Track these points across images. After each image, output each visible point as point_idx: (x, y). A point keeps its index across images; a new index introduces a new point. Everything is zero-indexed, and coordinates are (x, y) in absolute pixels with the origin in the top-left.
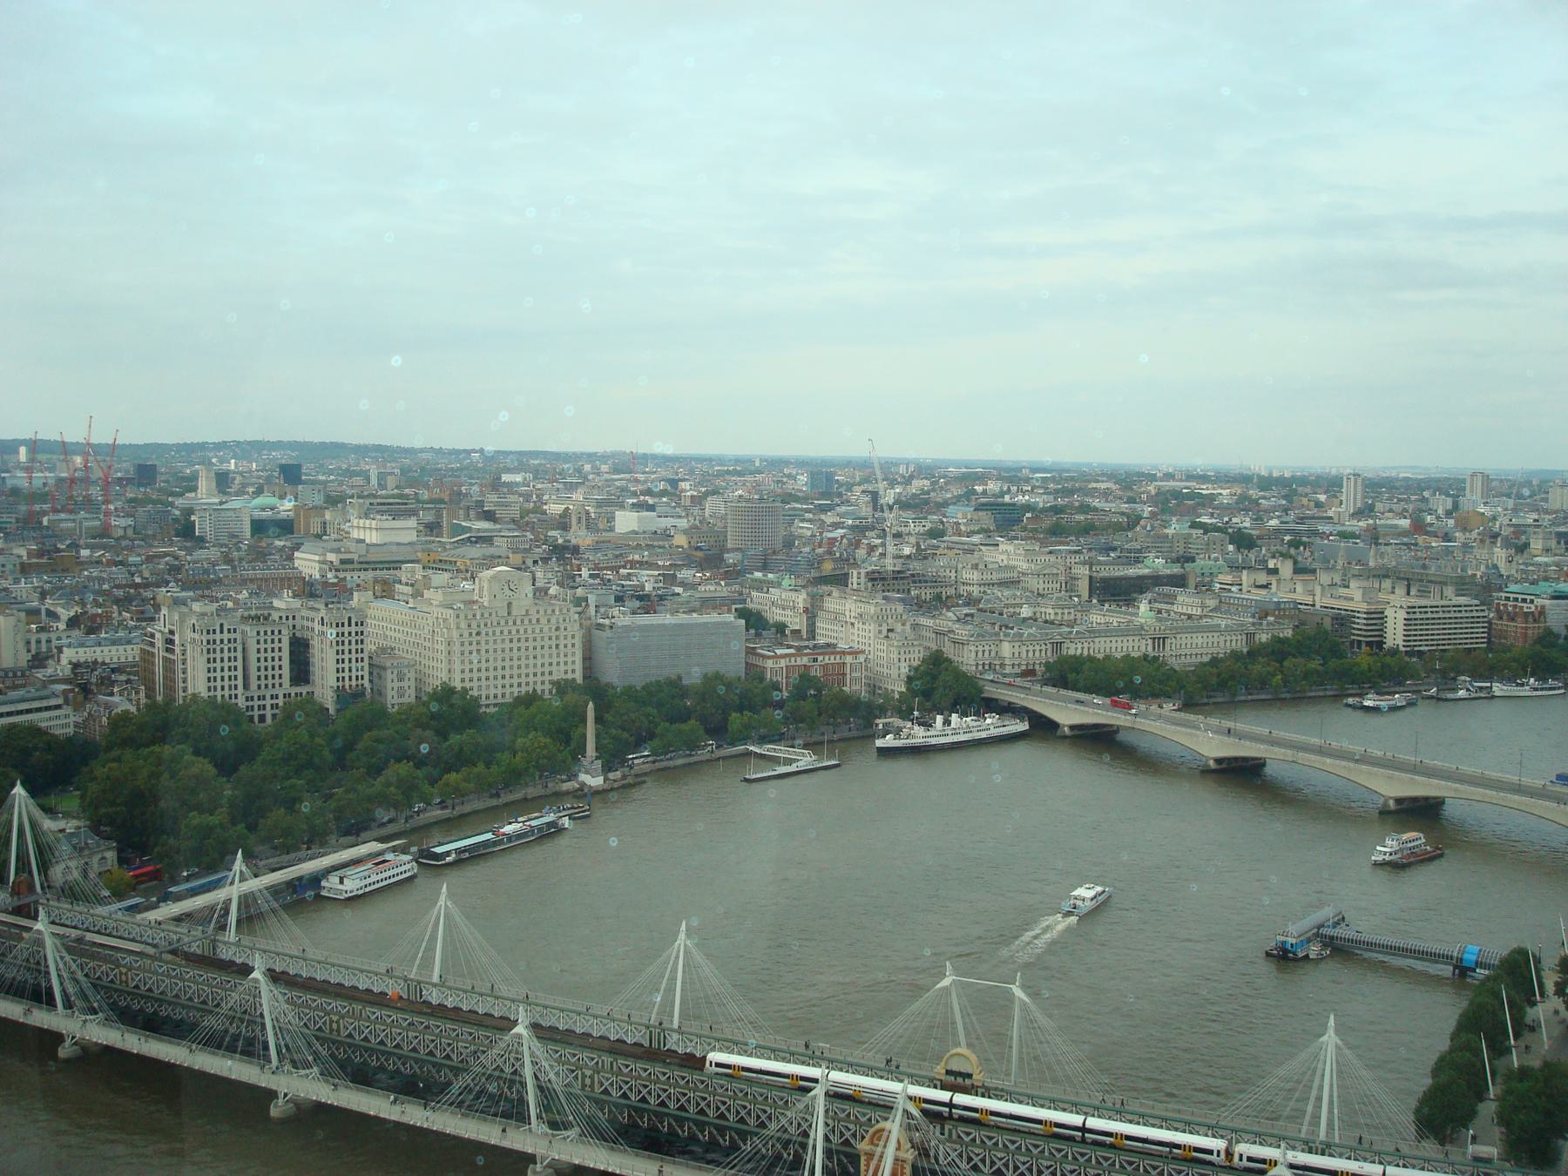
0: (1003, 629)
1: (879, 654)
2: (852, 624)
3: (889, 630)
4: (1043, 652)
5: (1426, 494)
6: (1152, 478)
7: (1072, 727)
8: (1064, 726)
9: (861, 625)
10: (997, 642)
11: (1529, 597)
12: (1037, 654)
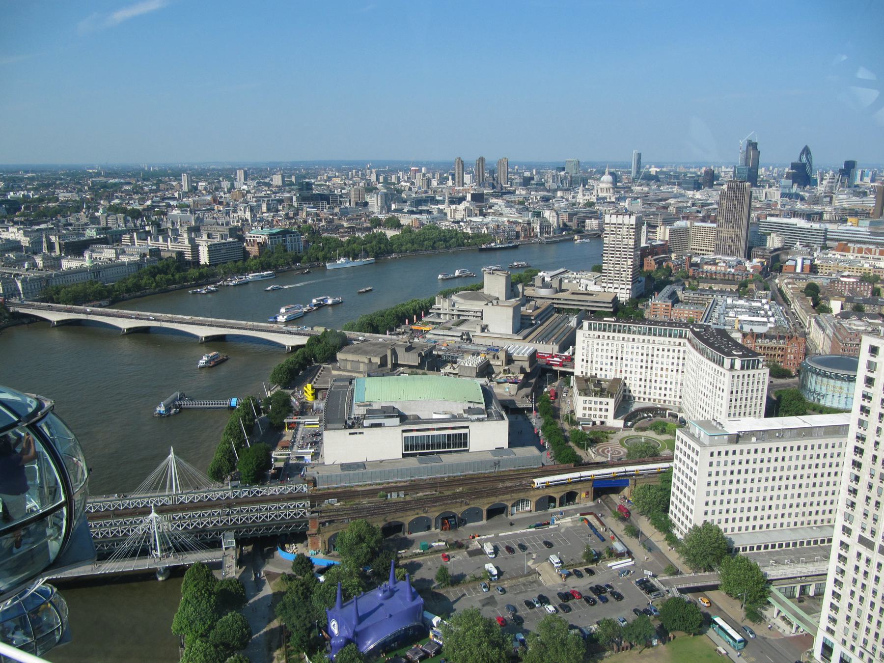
5: (221, 179)
6: (91, 175)
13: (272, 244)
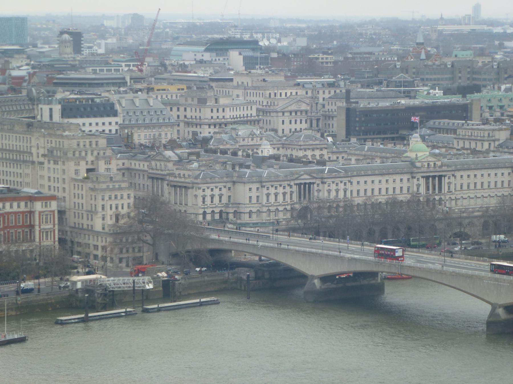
0: (237, 168)
1: (76, 201)
2: (42, 163)
3: (88, 171)
4: (288, 196)
7: (324, 279)
8: (313, 277)
9: (52, 165)
10: (229, 185)
12: (280, 198)
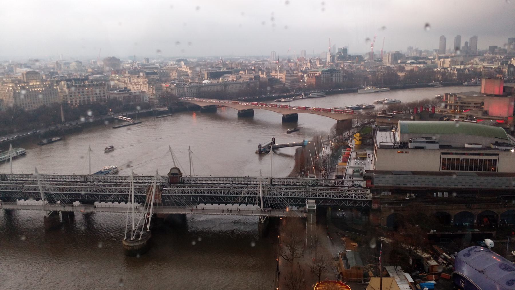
7: (204, 107)
11: (316, 72)
13: (324, 77)
